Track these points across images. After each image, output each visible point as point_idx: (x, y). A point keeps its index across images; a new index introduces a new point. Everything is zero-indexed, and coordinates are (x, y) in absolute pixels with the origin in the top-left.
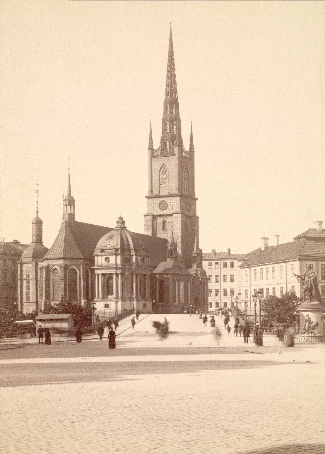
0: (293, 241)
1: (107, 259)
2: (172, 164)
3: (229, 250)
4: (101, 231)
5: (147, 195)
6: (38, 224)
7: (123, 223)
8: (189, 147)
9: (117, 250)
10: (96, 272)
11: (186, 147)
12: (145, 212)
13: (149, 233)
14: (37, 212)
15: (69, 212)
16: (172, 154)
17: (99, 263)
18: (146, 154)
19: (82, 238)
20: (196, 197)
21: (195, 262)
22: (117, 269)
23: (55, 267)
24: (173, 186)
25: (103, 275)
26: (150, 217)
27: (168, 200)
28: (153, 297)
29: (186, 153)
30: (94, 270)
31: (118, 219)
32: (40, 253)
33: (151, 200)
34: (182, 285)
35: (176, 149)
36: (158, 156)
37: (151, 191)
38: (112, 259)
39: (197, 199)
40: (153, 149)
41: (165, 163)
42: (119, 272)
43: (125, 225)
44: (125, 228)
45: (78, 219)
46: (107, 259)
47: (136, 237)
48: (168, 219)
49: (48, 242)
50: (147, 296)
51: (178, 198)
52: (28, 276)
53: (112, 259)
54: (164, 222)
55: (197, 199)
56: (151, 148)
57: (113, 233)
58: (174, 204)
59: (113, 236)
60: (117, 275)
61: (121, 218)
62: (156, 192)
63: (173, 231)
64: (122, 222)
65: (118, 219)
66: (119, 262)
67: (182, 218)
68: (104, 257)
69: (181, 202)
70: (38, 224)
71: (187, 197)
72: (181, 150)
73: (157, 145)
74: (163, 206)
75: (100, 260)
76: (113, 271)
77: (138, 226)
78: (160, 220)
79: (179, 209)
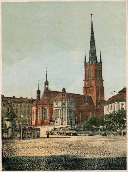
0: (118, 93)
1: (57, 104)
2: (93, 68)
6: (39, 92)
7: (65, 90)
10: (54, 109)
11: (99, 61)
18: (84, 64)
20: (103, 79)
22: (60, 107)
23: (40, 108)
25: (56, 110)
30: (53, 108)
40: (86, 63)
42: (61, 109)
46: (57, 104)
53: (59, 103)
55: (103, 80)
57: (60, 94)
60: (60, 110)
61: (64, 88)
64: (64, 90)
66: (61, 106)
70: (39, 92)
73: (87, 61)
76: (59, 109)
78: (88, 89)
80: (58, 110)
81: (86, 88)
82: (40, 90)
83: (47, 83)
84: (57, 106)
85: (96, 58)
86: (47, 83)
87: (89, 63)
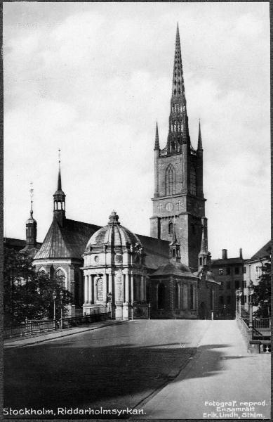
2: (179, 163)
7: (116, 218)
8: (197, 146)
9: (107, 247)
10: (86, 273)
11: (194, 146)
12: (152, 216)
14: (32, 213)
15: (60, 208)
18: (153, 154)
21: (201, 264)
22: (106, 267)
25: (93, 276)
26: (157, 220)
29: (194, 152)
33: (157, 204)
39: (206, 200)
40: (160, 150)
43: (119, 220)
45: (70, 215)
54: (170, 225)
55: (206, 200)
56: (157, 147)
60: (107, 275)
71: (196, 201)
72: (189, 149)
73: (163, 144)
75: (89, 260)
76: (103, 271)
77: (144, 228)
79: (185, 210)
80: (101, 275)
81: (159, 219)
83: (60, 197)
84: (94, 263)
85: (188, 138)
86: (60, 197)
87: (169, 149)
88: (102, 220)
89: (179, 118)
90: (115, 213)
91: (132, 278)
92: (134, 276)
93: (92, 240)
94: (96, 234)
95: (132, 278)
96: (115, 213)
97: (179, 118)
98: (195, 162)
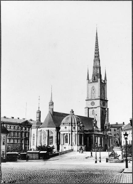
1: (66, 128)
2: (97, 86)
3: (124, 123)
4: (64, 115)
5: (86, 99)
7: (73, 112)
11: (103, 78)
13: (87, 116)
16: (97, 81)
17: (62, 130)
19: (57, 118)
24: (97, 95)
25: (64, 134)
26: (87, 109)
27: (94, 101)
28: (84, 144)
31: (71, 111)
32: (39, 124)
34: (99, 138)
35: (99, 80)
36: (91, 83)
37: (88, 97)
38: (68, 127)
41: (94, 86)
44: (74, 114)
45: (54, 111)
47: (79, 117)
48: (95, 110)
49: (42, 120)
50: (82, 144)
51: (99, 100)
52: (34, 134)
53: (68, 127)
58: (98, 103)
59: (68, 118)
60: (70, 134)
62: (90, 98)
63: (97, 115)
65: (71, 111)
67: (101, 109)
68: (65, 127)
69: (100, 102)
71: (104, 101)
73: (91, 77)
74: (93, 104)
75: (62, 128)
76: (68, 133)
78: (90, 110)
79: (99, 105)
80: (67, 134)
81: (89, 108)
82: (40, 110)
85: (101, 75)
86: (52, 104)
88: (68, 112)
89: (97, 68)
90: (72, 110)
91: (79, 135)
92: (80, 134)
93: (64, 121)
94: (65, 118)
95: (79, 135)
96: (72, 110)
97: (97, 68)
98: (103, 85)
